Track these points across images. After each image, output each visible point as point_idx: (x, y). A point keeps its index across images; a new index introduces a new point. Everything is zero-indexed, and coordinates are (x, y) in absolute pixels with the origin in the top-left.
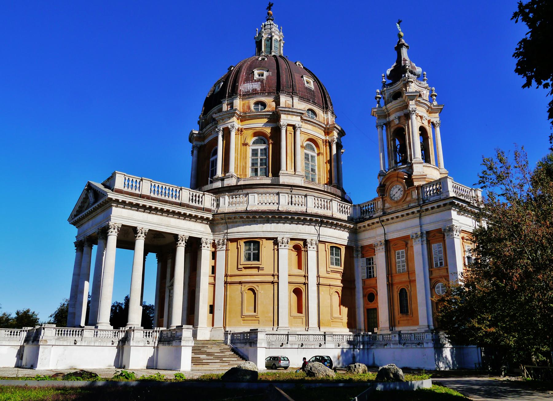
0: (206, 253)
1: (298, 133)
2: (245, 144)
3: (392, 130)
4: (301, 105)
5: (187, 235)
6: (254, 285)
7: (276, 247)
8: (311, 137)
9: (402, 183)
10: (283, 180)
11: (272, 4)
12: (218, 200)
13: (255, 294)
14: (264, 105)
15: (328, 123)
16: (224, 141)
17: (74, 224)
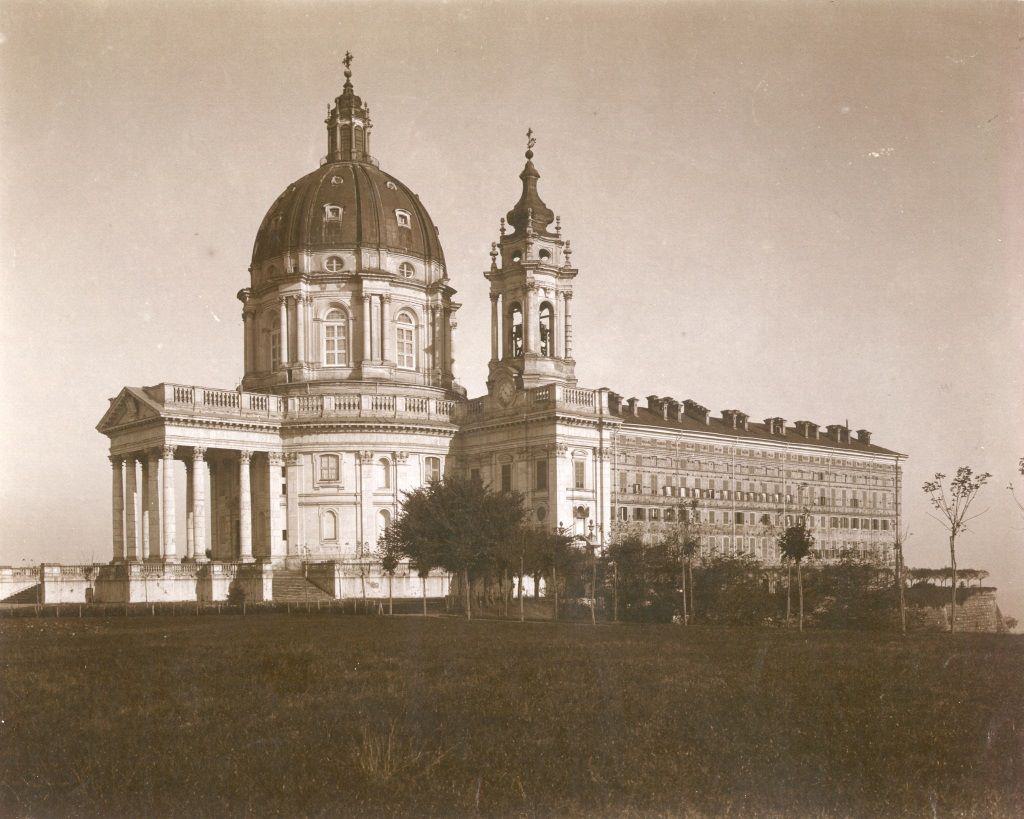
0: (275, 472)
1: (386, 306)
2: (317, 320)
3: (507, 303)
4: (391, 263)
5: (252, 449)
6: (334, 508)
7: (358, 461)
8: (406, 304)
9: (511, 381)
10: (369, 371)
11: (352, 57)
12: (286, 403)
13: (335, 516)
14: (340, 261)
15: (430, 281)
16: (290, 313)
17: (104, 433)
